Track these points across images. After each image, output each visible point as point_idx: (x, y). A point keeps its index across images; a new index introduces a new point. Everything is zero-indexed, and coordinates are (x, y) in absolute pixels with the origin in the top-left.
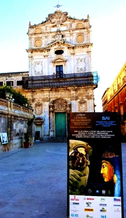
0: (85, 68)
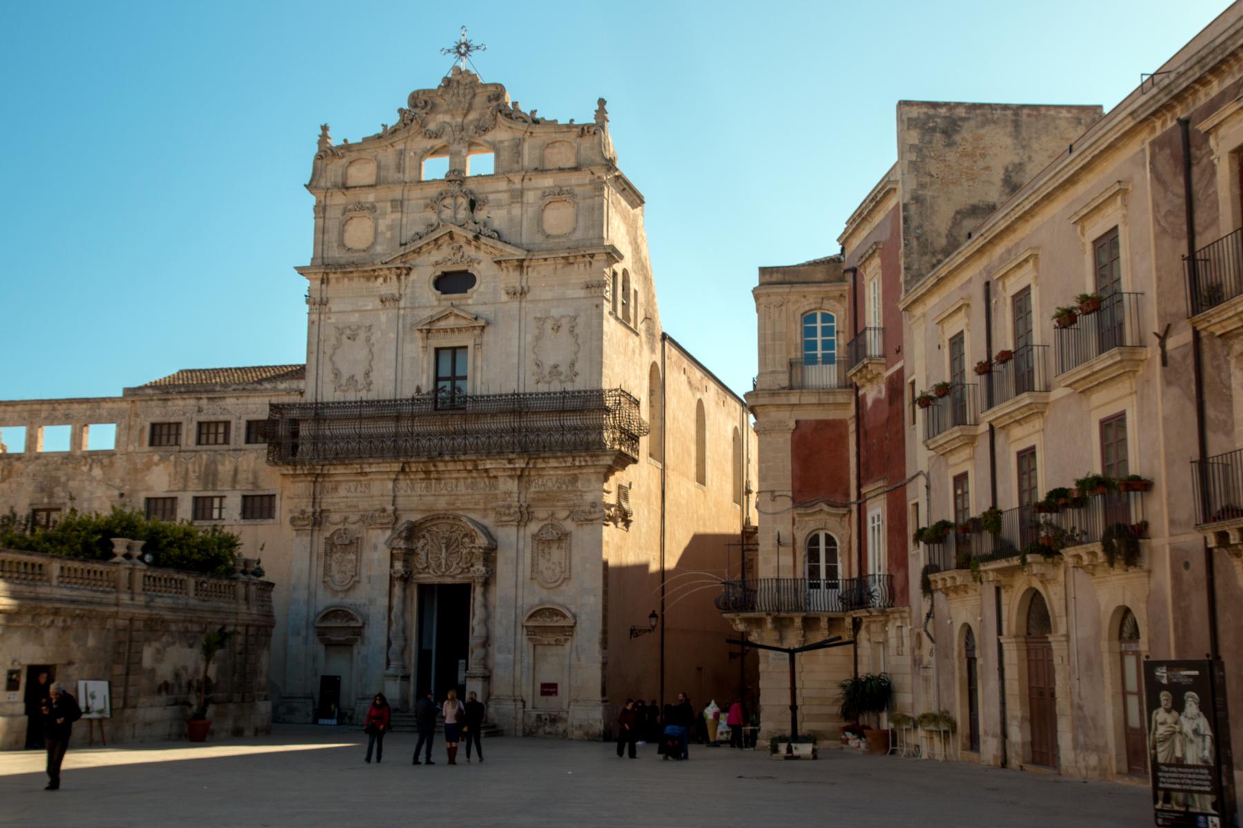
0: (573, 364)
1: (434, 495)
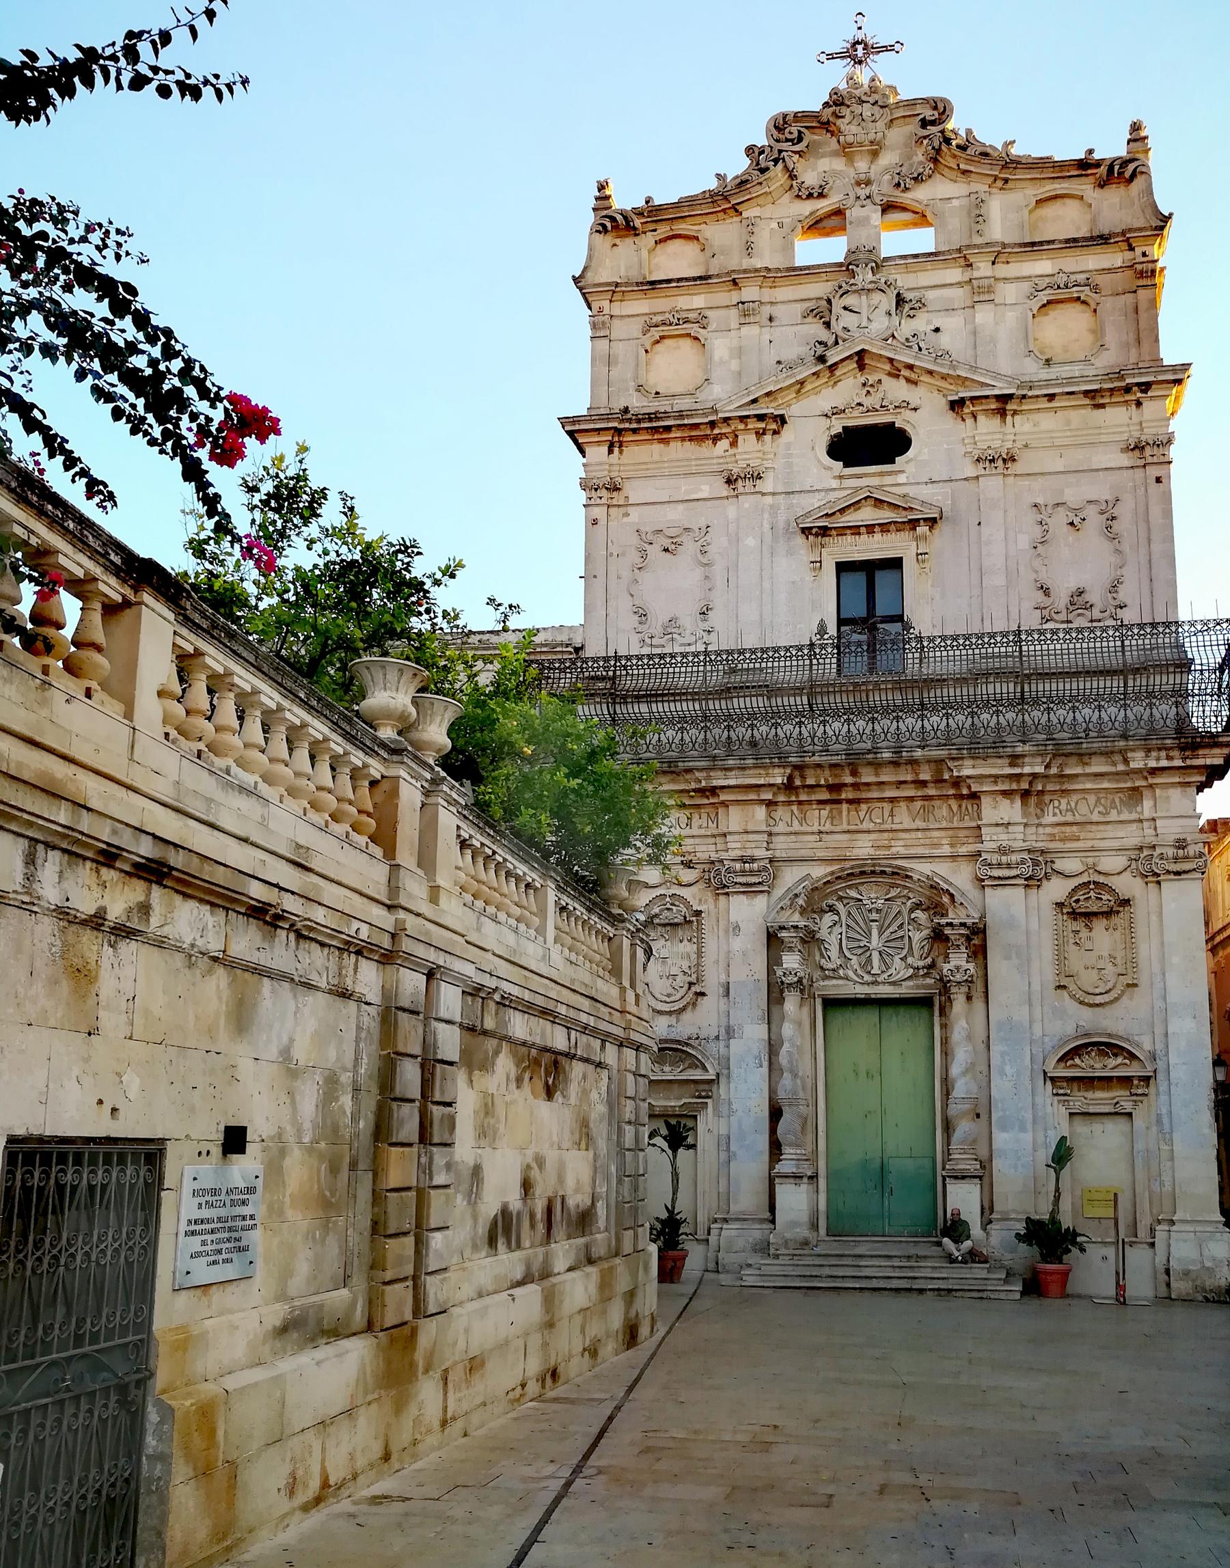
0: (1114, 589)
1: (848, 832)
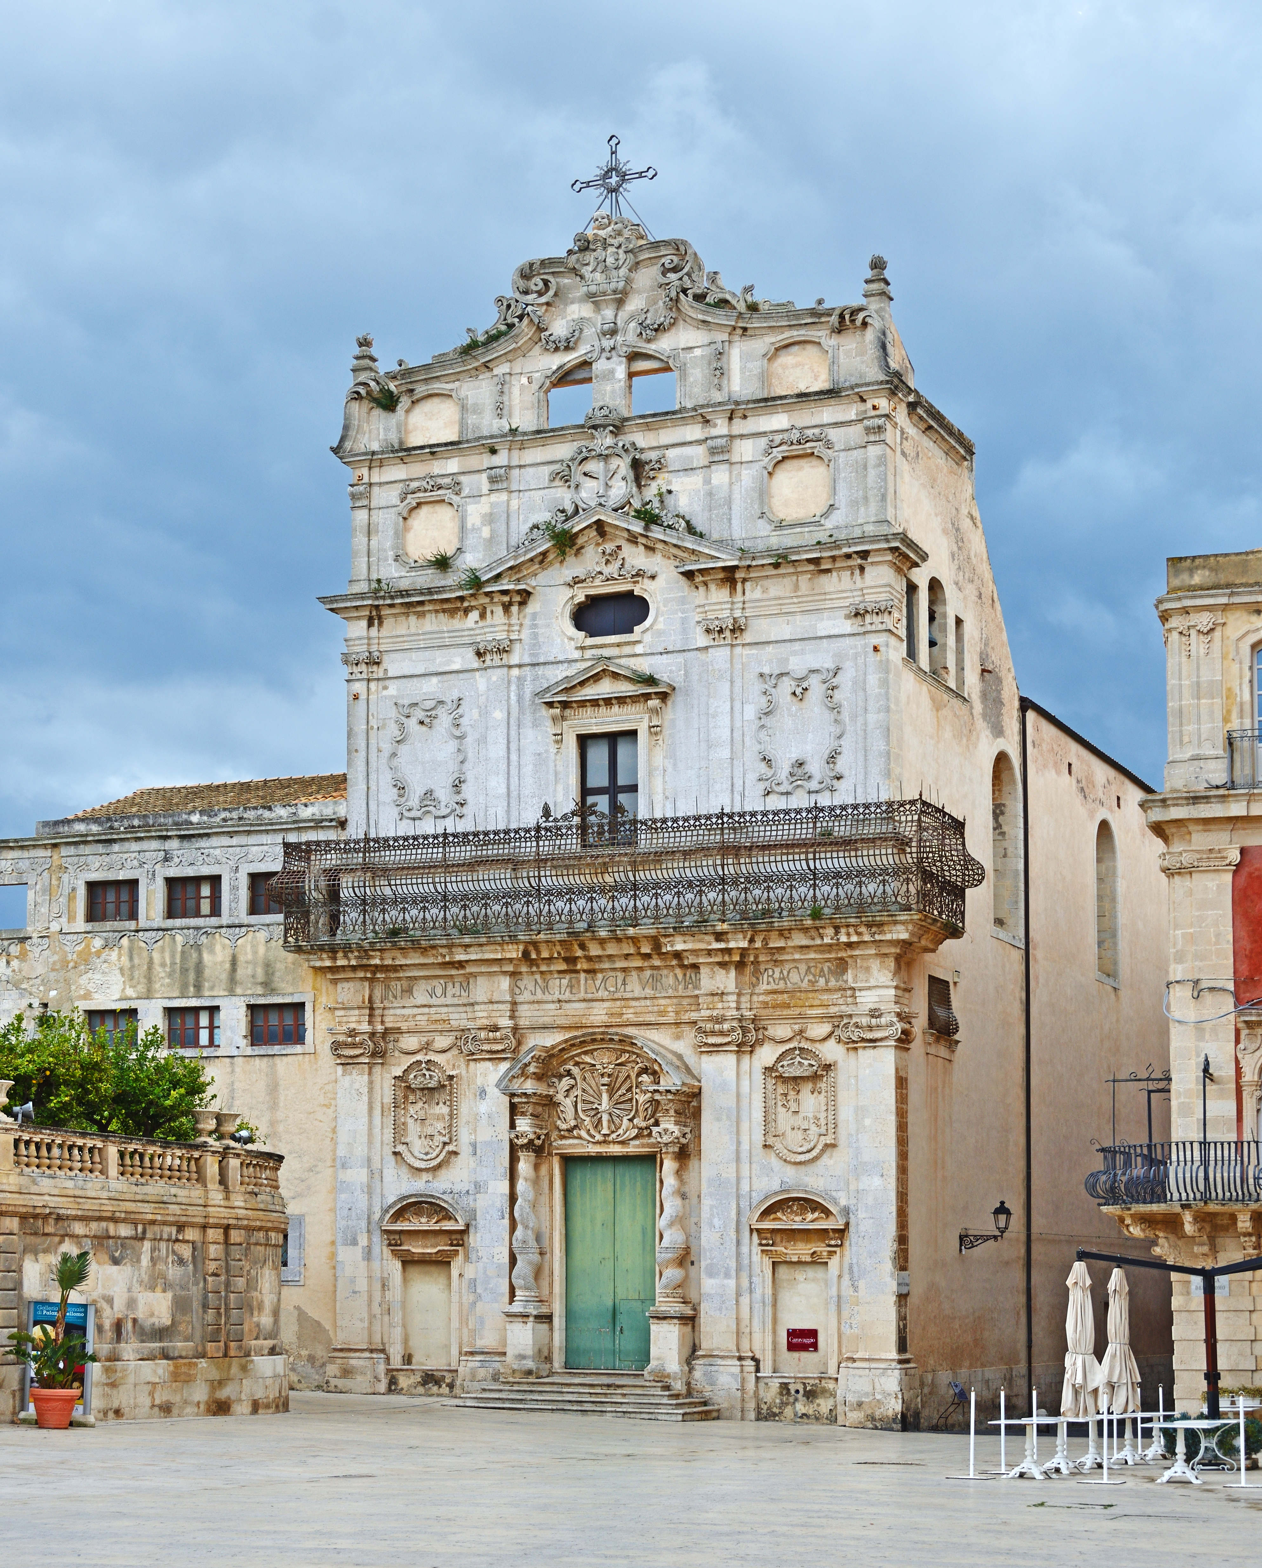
1: (584, 1000)
